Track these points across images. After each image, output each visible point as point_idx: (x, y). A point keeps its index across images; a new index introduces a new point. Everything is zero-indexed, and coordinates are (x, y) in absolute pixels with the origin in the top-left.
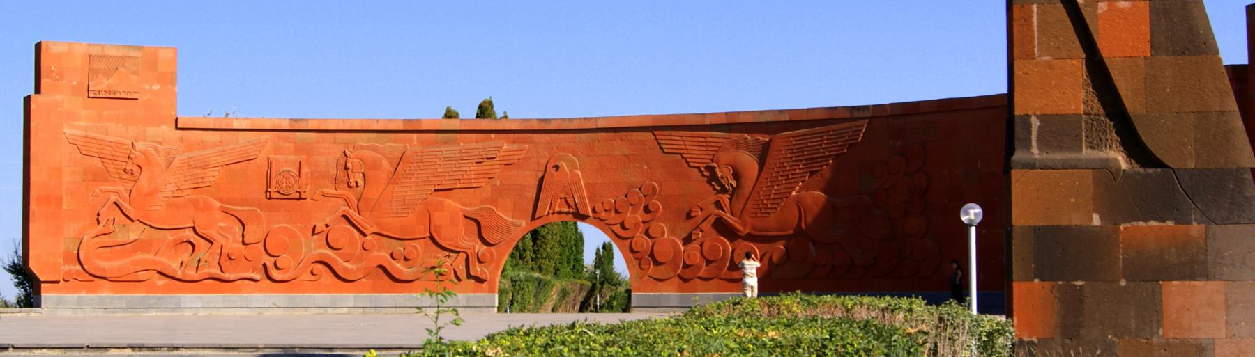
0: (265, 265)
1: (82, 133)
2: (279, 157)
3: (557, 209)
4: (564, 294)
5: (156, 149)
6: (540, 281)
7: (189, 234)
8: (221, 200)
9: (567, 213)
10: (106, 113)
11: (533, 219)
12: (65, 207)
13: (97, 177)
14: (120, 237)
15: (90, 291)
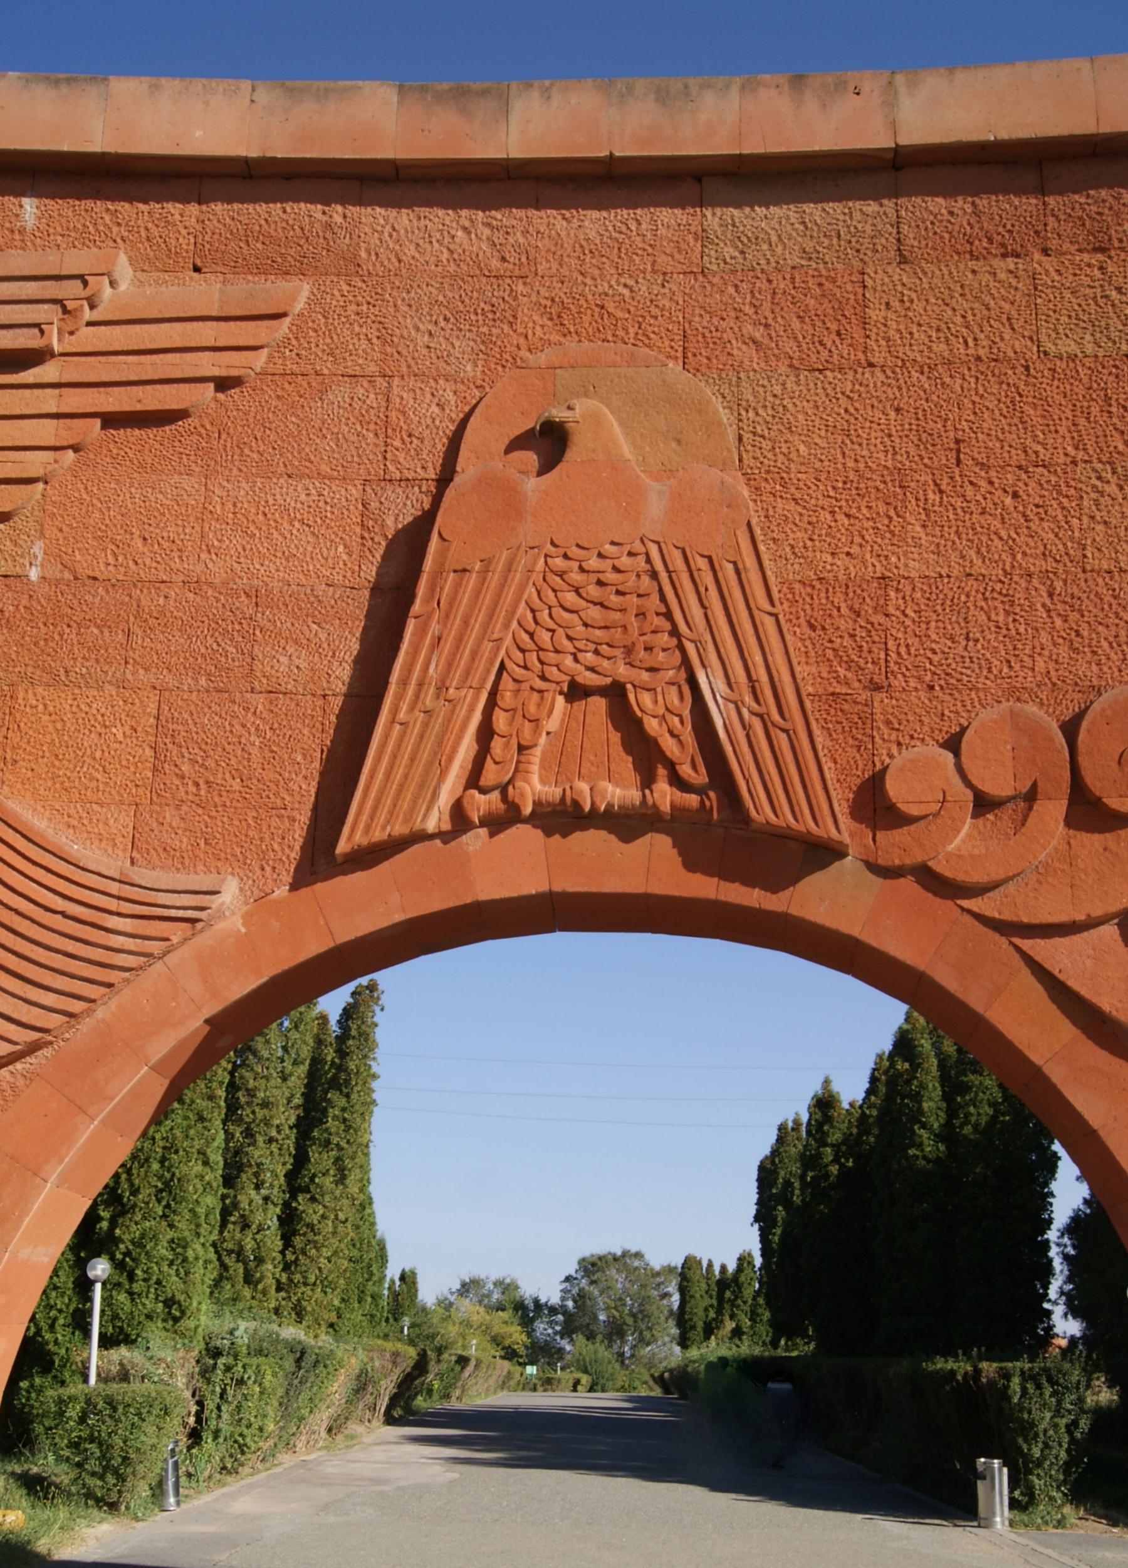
3: (536, 787)
4: (362, 1384)
6: (300, 1354)
9: (626, 824)
11: (319, 860)
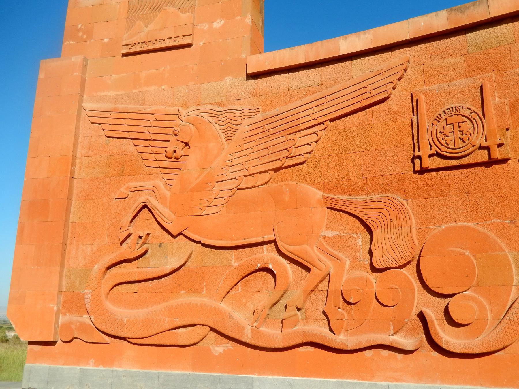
0: (421, 316)
1: (109, 106)
2: (436, 88)
5: (216, 117)
7: (267, 256)
8: (326, 187)
10: (144, 74)
12: (73, 218)
13: (125, 168)
14: (154, 265)
15: (102, 361)
